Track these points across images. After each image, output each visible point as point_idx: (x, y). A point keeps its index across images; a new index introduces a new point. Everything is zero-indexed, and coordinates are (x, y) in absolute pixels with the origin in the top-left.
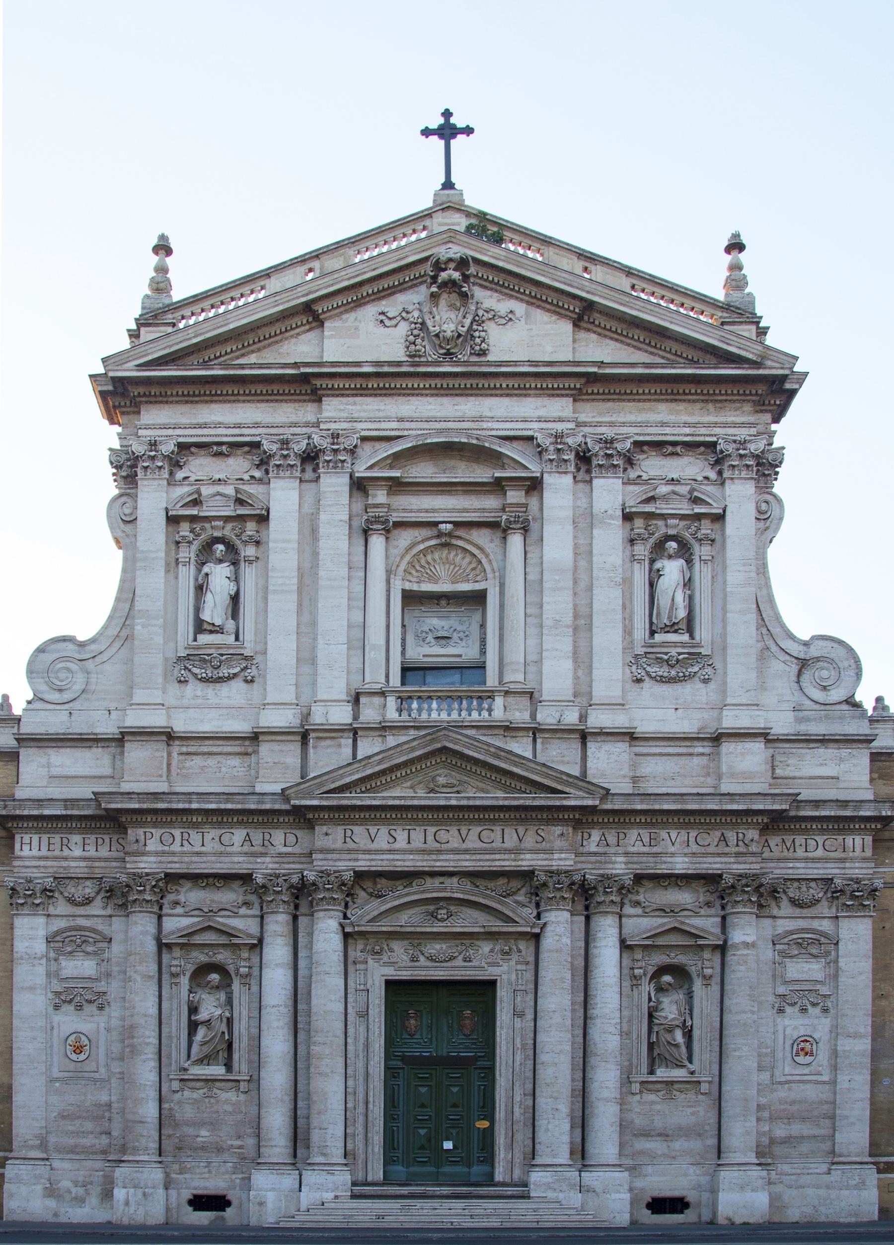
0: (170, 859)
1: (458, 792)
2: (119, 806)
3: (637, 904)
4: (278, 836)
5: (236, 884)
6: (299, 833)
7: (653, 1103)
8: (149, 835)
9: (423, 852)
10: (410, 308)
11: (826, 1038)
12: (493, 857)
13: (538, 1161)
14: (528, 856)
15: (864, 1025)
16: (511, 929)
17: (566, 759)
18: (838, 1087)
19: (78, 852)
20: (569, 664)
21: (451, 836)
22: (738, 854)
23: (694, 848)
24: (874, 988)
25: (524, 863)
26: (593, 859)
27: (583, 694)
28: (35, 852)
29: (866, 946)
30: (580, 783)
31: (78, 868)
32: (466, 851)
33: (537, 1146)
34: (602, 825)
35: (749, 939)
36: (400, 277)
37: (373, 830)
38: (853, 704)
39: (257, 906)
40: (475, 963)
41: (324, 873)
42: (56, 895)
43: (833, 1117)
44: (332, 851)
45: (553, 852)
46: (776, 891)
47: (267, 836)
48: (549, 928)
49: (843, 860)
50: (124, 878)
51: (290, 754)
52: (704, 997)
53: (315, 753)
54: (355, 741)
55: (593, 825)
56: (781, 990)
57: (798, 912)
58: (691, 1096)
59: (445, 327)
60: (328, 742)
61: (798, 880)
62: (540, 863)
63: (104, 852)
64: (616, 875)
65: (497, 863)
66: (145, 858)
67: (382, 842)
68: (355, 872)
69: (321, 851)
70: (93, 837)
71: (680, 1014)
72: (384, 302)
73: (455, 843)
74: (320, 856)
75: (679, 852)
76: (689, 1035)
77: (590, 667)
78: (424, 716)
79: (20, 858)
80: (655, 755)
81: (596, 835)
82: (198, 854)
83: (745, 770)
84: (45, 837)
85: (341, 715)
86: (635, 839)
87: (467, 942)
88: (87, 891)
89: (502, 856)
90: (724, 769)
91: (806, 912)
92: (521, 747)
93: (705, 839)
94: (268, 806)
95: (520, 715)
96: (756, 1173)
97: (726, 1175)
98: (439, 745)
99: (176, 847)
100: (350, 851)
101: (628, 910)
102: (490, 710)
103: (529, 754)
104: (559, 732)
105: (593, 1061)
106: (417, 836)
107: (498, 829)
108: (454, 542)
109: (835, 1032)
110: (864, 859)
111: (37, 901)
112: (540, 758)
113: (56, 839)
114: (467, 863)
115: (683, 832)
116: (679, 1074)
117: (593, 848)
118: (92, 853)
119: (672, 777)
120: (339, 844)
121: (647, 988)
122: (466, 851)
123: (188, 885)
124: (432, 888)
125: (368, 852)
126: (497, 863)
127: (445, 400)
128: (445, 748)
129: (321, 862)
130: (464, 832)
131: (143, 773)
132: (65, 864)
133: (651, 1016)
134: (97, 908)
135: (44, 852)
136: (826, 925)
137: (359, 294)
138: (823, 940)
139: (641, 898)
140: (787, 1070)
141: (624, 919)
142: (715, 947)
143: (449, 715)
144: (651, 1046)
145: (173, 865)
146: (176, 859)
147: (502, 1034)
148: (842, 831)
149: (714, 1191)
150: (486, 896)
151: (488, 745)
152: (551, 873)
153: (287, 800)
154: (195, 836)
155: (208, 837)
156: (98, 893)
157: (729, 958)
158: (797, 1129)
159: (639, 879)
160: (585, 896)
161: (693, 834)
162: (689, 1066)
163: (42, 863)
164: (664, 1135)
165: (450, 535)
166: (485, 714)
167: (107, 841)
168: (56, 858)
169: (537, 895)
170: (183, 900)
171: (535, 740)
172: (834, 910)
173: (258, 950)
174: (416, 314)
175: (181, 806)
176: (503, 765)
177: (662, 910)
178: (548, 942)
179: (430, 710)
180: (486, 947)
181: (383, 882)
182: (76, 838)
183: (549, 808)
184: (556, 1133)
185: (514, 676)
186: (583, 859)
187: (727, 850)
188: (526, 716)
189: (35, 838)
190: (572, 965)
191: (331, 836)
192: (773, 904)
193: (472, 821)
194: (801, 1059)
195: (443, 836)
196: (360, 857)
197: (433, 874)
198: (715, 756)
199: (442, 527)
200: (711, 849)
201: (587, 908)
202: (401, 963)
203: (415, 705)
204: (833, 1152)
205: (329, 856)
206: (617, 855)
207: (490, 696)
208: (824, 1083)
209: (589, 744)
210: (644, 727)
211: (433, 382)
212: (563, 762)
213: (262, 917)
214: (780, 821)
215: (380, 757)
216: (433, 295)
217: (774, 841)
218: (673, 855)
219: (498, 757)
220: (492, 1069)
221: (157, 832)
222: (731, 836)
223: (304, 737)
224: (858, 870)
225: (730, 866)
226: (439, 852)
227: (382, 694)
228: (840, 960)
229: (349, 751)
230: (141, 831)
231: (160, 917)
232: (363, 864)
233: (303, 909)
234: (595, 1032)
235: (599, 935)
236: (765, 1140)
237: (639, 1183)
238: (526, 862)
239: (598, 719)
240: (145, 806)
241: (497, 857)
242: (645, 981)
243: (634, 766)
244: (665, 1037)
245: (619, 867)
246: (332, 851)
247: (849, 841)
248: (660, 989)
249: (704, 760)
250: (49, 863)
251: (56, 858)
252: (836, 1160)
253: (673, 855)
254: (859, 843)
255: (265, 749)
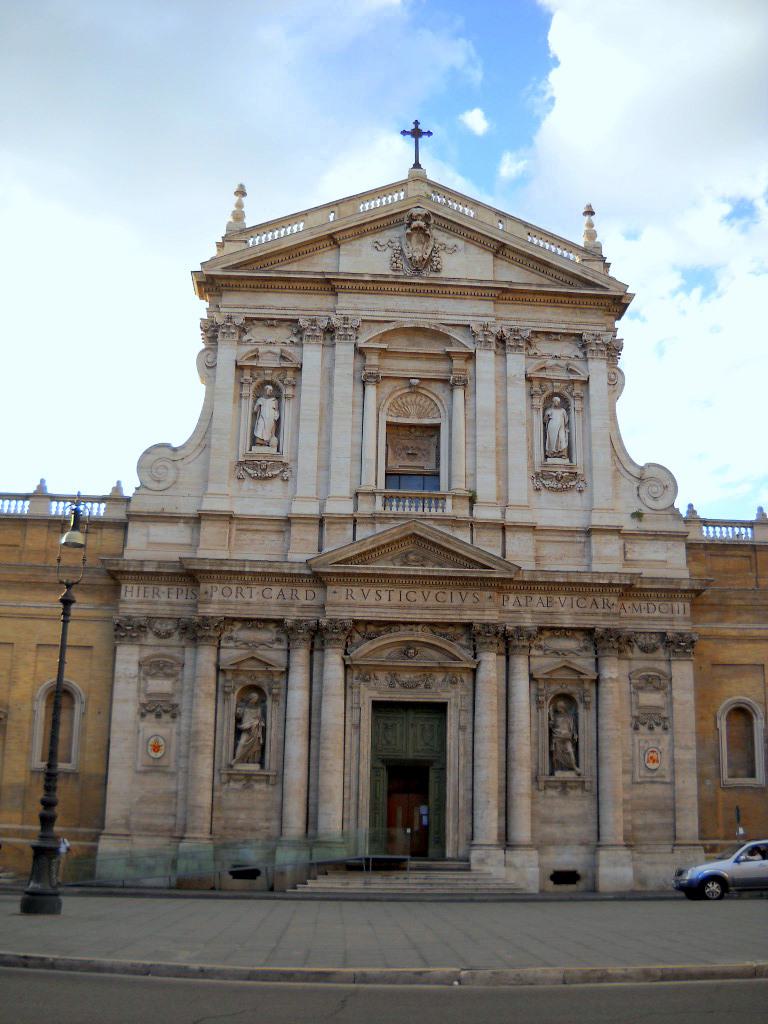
0: (227, 607)
1: (422, 565)
2: (196, 567)
3: (540, 647)
4: (301, 593)
5: (271, 626)
6: (316, 590)
7: (552, 797)
8: (214, 589)
9: (399, 607)
10: (393, 239)
11: (666, 749)
12: (444, 612)
13: (475, 842)
14: (468, 612)
15: (691, 741)
16: (457, 665)
17: (492, 544)
18: (676, 787)
19: (164, 598)
20: (493, 478)
21: (417, 596)
22: (604, 614)
23: (576, 609)
24: (697, 713)
25: (465, 617)
26: (510, 615)
27: (505, 504)
28: (134, 597)
29: (689, 681)
30: (502, 562)
31: (163, 610)
32: (427, 608)
33: (475, 830)
34: (517, 591)
35: (614, 676)
36: (388, 220)
37: (366, 590)
38: (676, 513)
39: (285, 642)
40: (433, 689)
41: (332, 621)
42: (148, 629)
43: (674, 810)
44: (338, 605)
45: (485, 610)
46: (630, 641)
47: (294, 593)
48: (483, 665)
49: (671, 619)
50: (197, 620)
51: (312, 534)
52: (585, 717)
53: (328, 534)
54: (355, 526)
55: (510, 590)
56: (636, 713)
57: (645, 655)
58: (579, 792)
59: (415, 254)
60: (338, 526)
61: (644, 633)
62: (476, 617)
63: (182, 599)
64: (526, 627)
65: (448, 617)
66: (212, 606)
67: (371, 599)
68: (354, 621)
69: (331, 605)
70: (175, 588)
71: (570, 731)
72: (377, 235)
73: (420, 601)
74: (331, 608)
75: (567, 612)
76: (576, 746)
77: (507, 479)
78: (400, 510)
79: (123, 602)
80: (549, 541)
81: (512, 597)
82: (248, 604)
83: (607, 559)
84: (142, 587)
85: (346, 508)
86: (537, 601)
87: (428, 674)
88: (169, 627)
89: (451, 612)
90: (594, 552)
91: (650, 656)
92: (463, 535)
93: (582, 603)
94: (296, 571)
95: (463, 512)
96: (624, 853)
97: (603, 854)
98: (409, 532)
99: (232, 598)
100: (350, 605)
101: (534, 652)
102: (443, 508)
103: (468, 541)
104: (487, 525)
105: (513, 765)
106: (395, 596)
107: (448, 592)
108: (420, 390)
109: (672, 744)
110: (685, 619)
111: (134, 635)
112: (476, 544)
113: (150, 588)
114: (429, 617)
115: (569, 597)
116: (568, 775)
117: (511, 607)
118: (173, 598)
119: (562, 561)
120: (343, 600)
121: (547, 710)
122: (427, 608)
123: (238, 625)
124: (404, 635)
125: (364, 606)
126: (448, 617)
127: (415, 299)
128: (414, 534)
129: (331, 613)
130: (426, 593)
131: (213, 546)
132: (155, 607)
133: (551, 732)
134: (175, 639)
135: (141, 598)
136: (663, 666)
137: (361, 230)
138: (661, 676)
139: (542, 643)
140: (642, 773)
141: (532, 659)
142: (593, 681)
143: (417, 510)
144: (551, 754)
145: (230, 611)
146: (232, 607)
147: (451, 743)
148: (670, 599)
149: (595, 866)
150: (440, 641)
151: (442, 533)
152: (486, 625)
153: (309, 567)
154: (246, 591)
155: (255, 591)
156: (176, 629)
157: (602, 689)
158: (652, 818)
159: (541, 630)
160: (507, 641)
161: (575, 599)
162: (577, 769)
163: (139, 606)
164: (562, 822)
165: (417, 386)
166: (440, 511)
167: (185, 592)
168: (150, 603)
169: (474, 641)
170: (235, 636)
171: (472, 530)
172: (667, 655)
173: (284, 677)
174: (398, 244)
175: (238, 569)
176: (452, 548)
177: (556, 652)
178: (481, 675)
179: (404, 507)
180: (440, 677)
181: (371, 628)
182: (164, 588)
183: (482, 579)
184: (488, 823)
185: (460, 486)
186: (505, 615)
187: (597, 611)
188: (466, 513)
189: (136, 587)
190: (498, 691)
191: (337, 594)
192: (628, 649)
193: (431, 586)
194: (652, 766)
195: (412, 596)
196: (356, 609)
197: (405, 623)
198: (588, 544)
199: (413, 381)
200: (587, 610)
201: (507, 650)
202: (379, 689)
203: (394, 503)
204: (675, 837)
205: (337, 608)
206: (524, 612)
207: (444, 498)
208: (666, 783)
209: (507, 534)
210: (542, 522)
211: (408, 287)
212: (490, 546)
213: (289, 651)
214: (629, 590)
215: (372, 539)
216: (407, 234)
217: (628, 604)
218: (563, 614)
219: (449, 542)
220: (443, 769)
221: (220, 587)
222: (599, 600)
223: (321, 521)
224: (683, 627)
225: (601, 623)
226: (410, 608)
227: (373, 494)
228: (673, 691)
229: (350, 532)
230: (209, 586)
231: (219, 649)
232: (359, 615)
233: (317, 646)
234: (514, 741)
235: (516, 671)
236: (629, 827)
237: (546, 859)
238: (468, 616)
239: (513, 517)
240: (214, 568)
241: (448, 612)
242: (546, 705)
243: (536, 550)
244: (559, 748)
245: (528, 622)
246: (338, 605)
247: (675, 605)
248: (556, 712)
249: (579, 547)
250: (144, 606)
251: (150, 603)
252: (677, 842)
253: (563, 614)
254: (681, 607)
255: (294, 529)
